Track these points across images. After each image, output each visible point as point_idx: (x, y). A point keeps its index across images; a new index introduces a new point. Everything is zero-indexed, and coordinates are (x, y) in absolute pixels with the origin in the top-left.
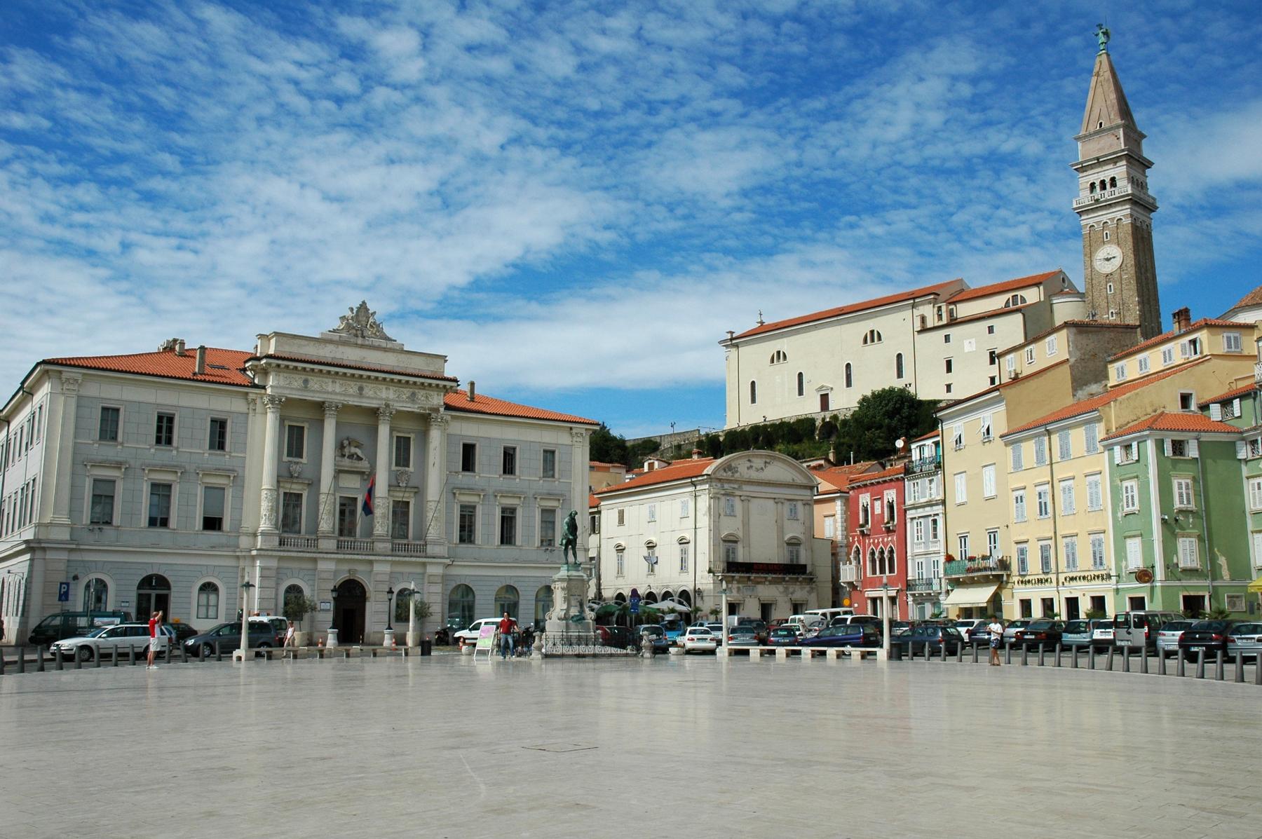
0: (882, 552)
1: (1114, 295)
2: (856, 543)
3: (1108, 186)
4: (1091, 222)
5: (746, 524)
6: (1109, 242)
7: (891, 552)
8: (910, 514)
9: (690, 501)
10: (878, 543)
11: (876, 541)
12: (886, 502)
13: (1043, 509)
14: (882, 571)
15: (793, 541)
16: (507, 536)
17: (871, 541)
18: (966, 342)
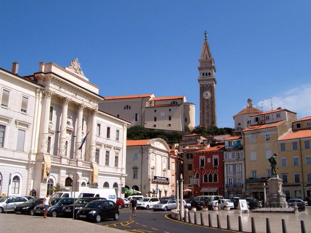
0: (210, 176)
1: (208, 105)
2: (197, 172)
3: (208, 74)
4: (203, 84)
5: (156, 163)
6: (208, 90)
7: (215, 176)
8: (225, 164)
9: (139, 153)
10: (209, 172)
11: (208, 171)
12: (213, 159)
13: (295, 163)
14: (211, 181)
15: (164, 170)
16: (107, 163)
17: (205, 171)
18: (162, 113)
